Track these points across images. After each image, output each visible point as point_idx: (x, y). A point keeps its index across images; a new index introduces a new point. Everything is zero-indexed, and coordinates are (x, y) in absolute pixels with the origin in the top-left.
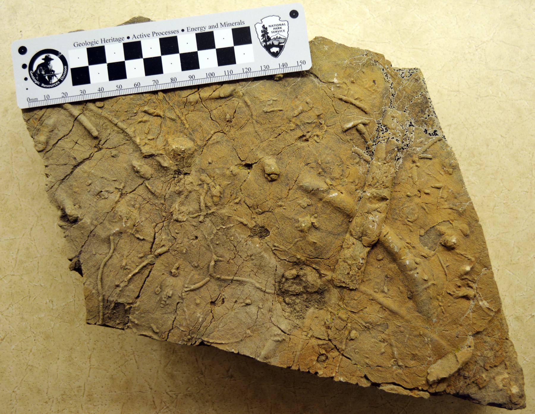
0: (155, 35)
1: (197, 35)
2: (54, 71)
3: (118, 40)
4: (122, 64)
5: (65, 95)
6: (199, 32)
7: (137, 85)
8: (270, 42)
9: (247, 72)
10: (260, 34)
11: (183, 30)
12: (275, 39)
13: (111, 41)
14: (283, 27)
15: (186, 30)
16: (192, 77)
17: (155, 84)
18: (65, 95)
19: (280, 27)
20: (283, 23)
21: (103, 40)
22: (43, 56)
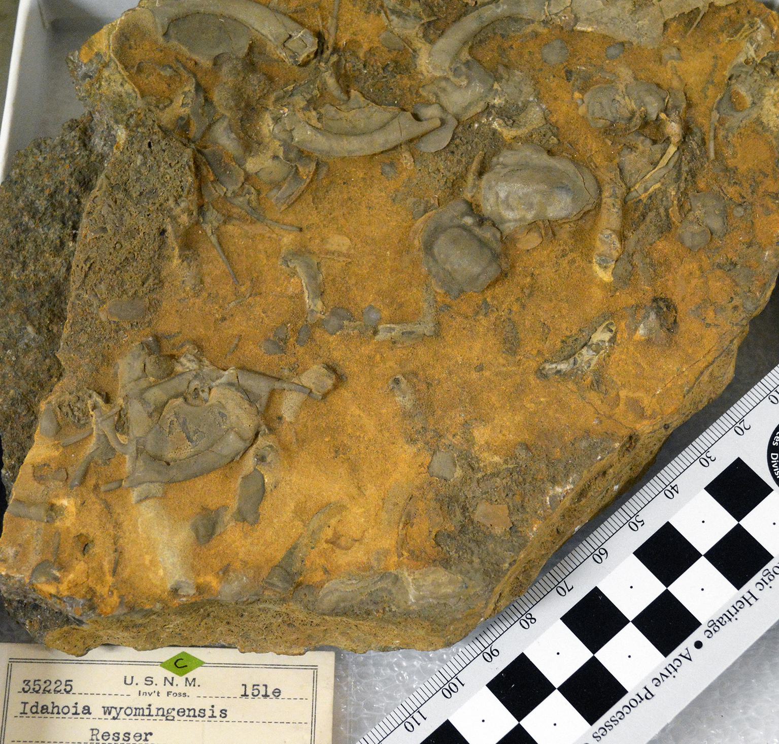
0: (643, 693)
3: (716, 625)
4: (667, 578)
5: (740, 428)
7: (600, 554)
13: (733, 611)
16: (491, 655)
17: (562, 585)
18: (740, 428)
21: (752, 600)
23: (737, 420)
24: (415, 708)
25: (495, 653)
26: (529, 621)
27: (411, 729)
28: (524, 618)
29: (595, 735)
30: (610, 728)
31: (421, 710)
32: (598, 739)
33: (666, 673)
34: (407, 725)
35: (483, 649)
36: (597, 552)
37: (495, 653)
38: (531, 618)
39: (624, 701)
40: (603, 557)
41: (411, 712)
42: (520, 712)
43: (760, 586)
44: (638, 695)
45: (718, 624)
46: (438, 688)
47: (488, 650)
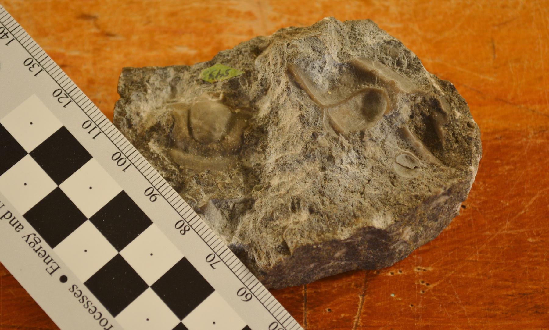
1: (53, 244)
6: (44, 244)
7: (246, 295)
9: (67, 95)
15: (58, 274)
16: (151, 195)
24: (103, 129)
25: (153, 198)
26: (183, 228)
27: (85, 126)
28: (186, 224)
29: (75, 287)
30: (81, 301)
31: (102, 134)
32: (72, 290)
34: (88, 123)
35: (157, 187)
36: (248, 292)
37: (153, 198)
38: (185, 231)
39: (106, 314)
40: (243, 297)
41: (100, 126)
42: (99, 220)
44: (112, 326)
46: (121, 148)
47: (155, 192)
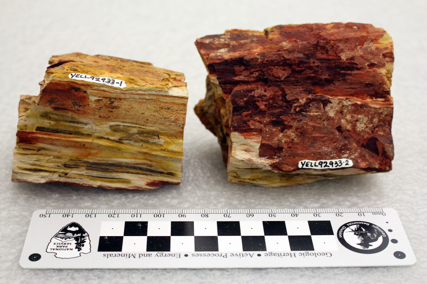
2: (355, 234)
3: (271, 254)
8: (75, 235)
10: (86, 244)
11: (186, 255)
12: (69, 238)
13: (283, 254)
14: (55, 247)
19: (59, 248)
20: (52, 251)
22: (370, 248)
23: (340, 212)
33: (238, 255)
43: (300, 255)
45: (273, 254)
